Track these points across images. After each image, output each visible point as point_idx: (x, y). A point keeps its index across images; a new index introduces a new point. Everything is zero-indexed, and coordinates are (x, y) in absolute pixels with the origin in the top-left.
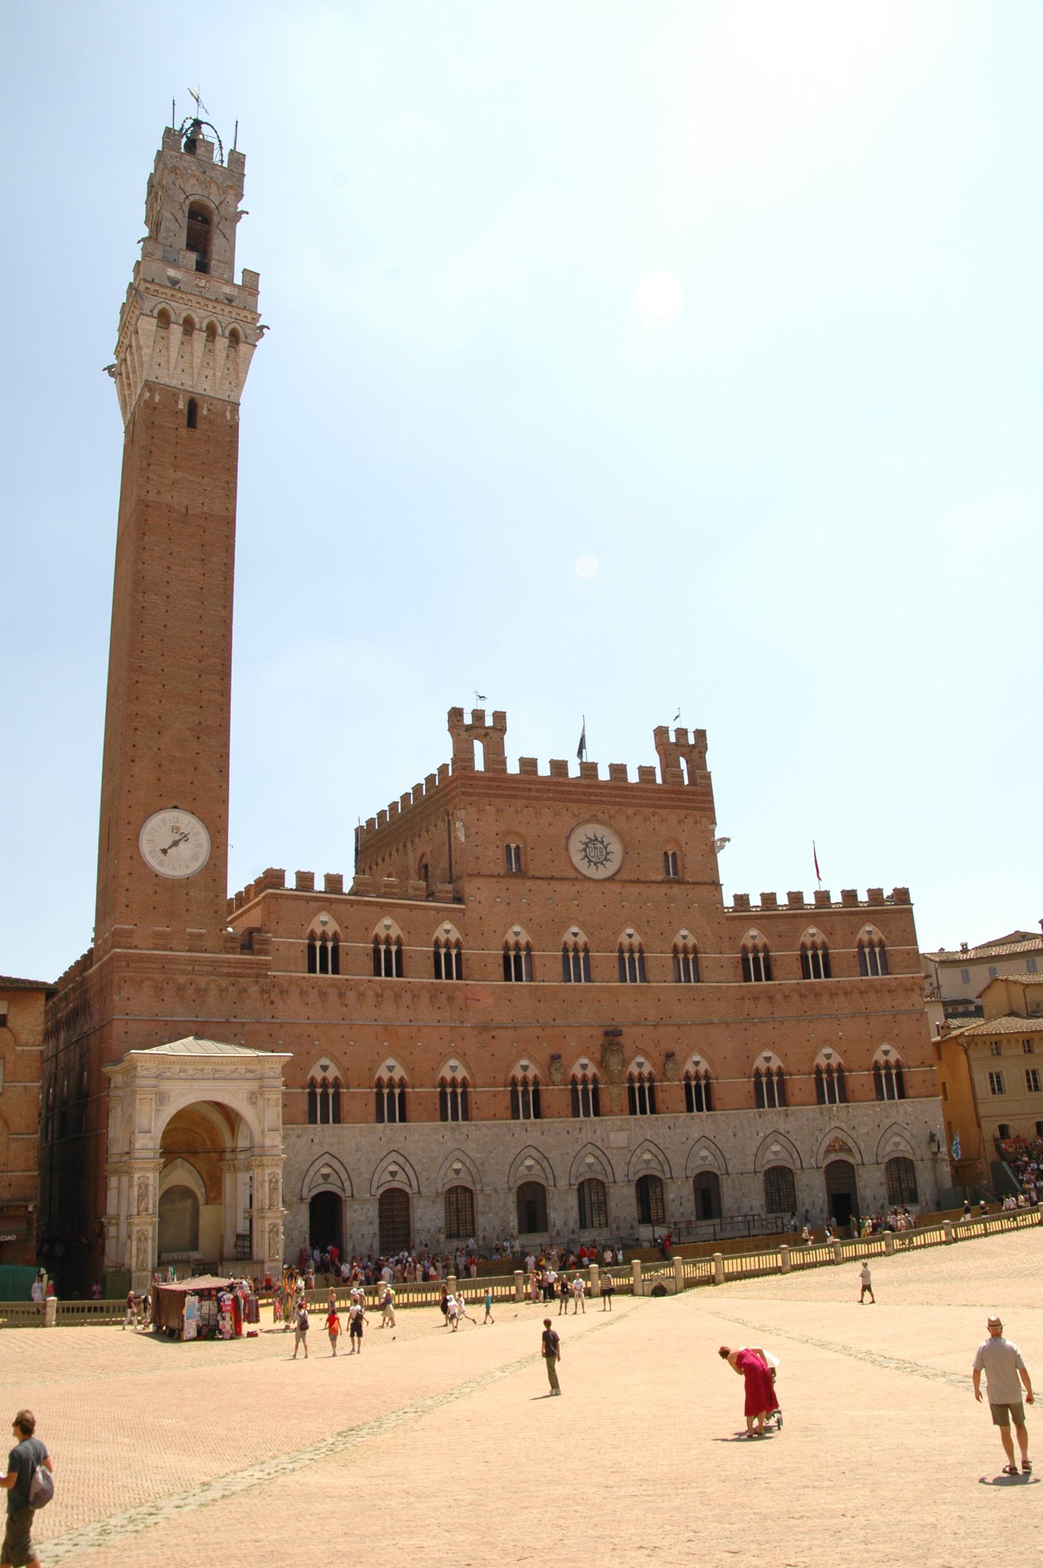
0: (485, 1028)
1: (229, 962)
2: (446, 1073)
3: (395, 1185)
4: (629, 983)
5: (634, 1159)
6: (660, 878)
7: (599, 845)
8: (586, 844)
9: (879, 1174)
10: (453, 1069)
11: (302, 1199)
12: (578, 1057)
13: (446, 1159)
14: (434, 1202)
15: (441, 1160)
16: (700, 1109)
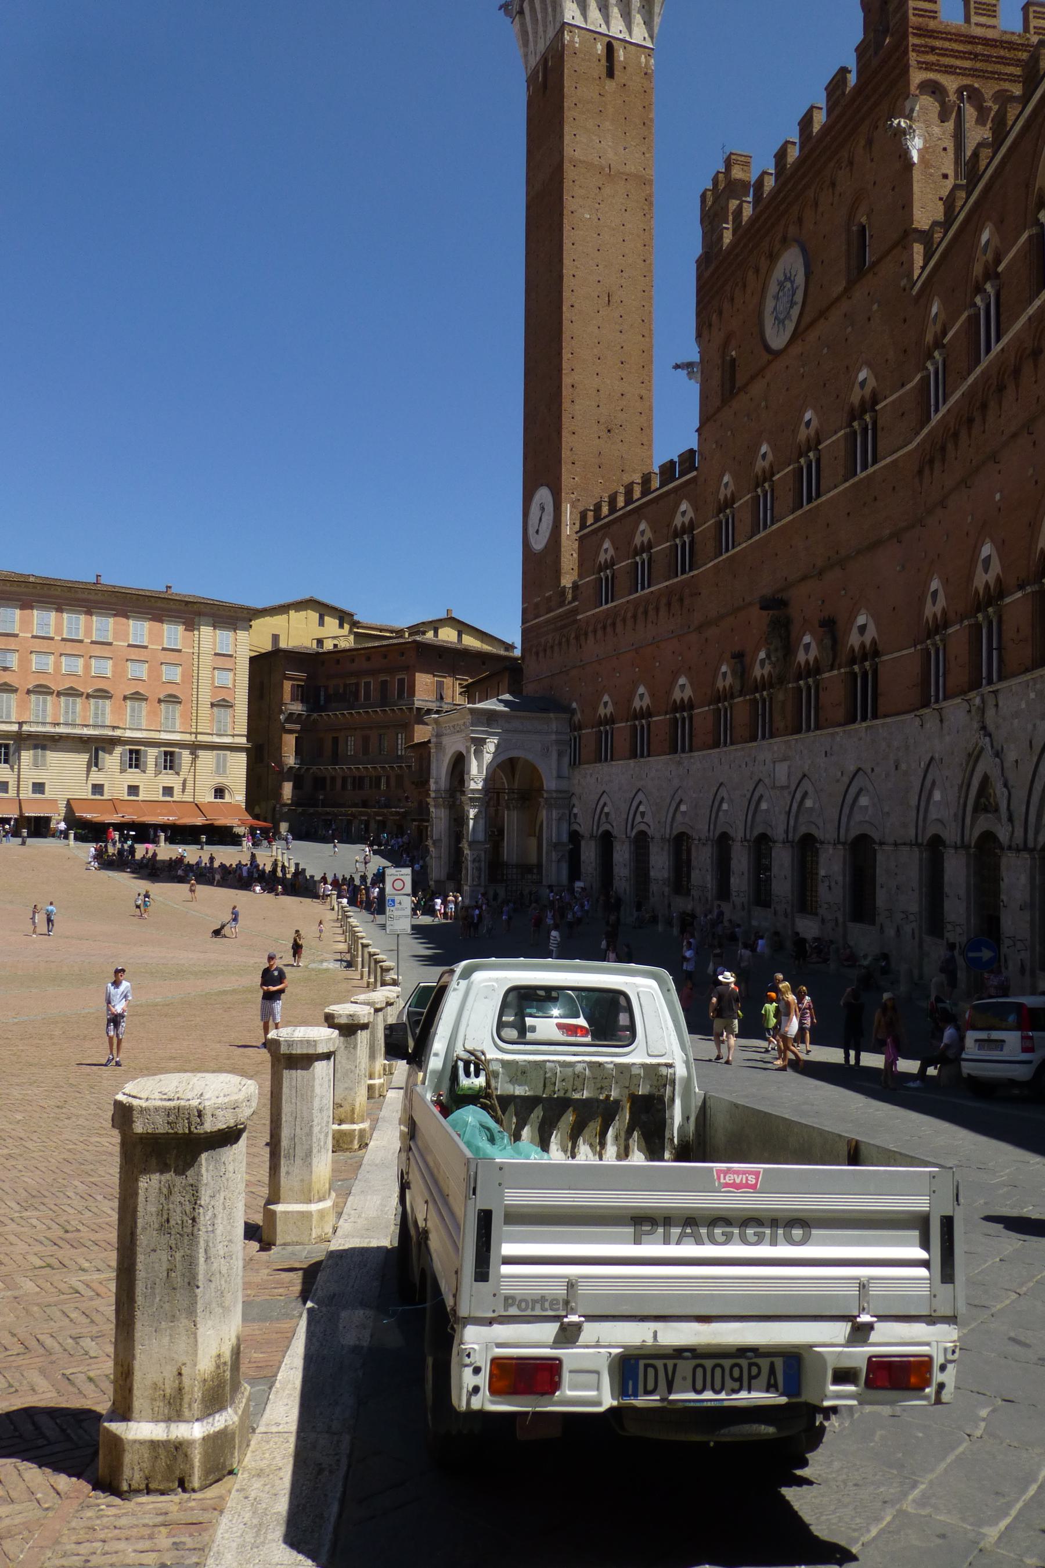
0: (700, 628)
1: (560, 617)
2: (677, 695)
3: (643, 827)
4: (806, 508)
5: (795, 805)
6: (841, 289)
7: (788, 285)
8: (777, 297)
9: (1024, 879)
10: (683, 689)
11: (592, 836)
12: (757, 650)
13: (673, 798)
14: (662, 849)
15: (668, 800)
16: (864, 719)
